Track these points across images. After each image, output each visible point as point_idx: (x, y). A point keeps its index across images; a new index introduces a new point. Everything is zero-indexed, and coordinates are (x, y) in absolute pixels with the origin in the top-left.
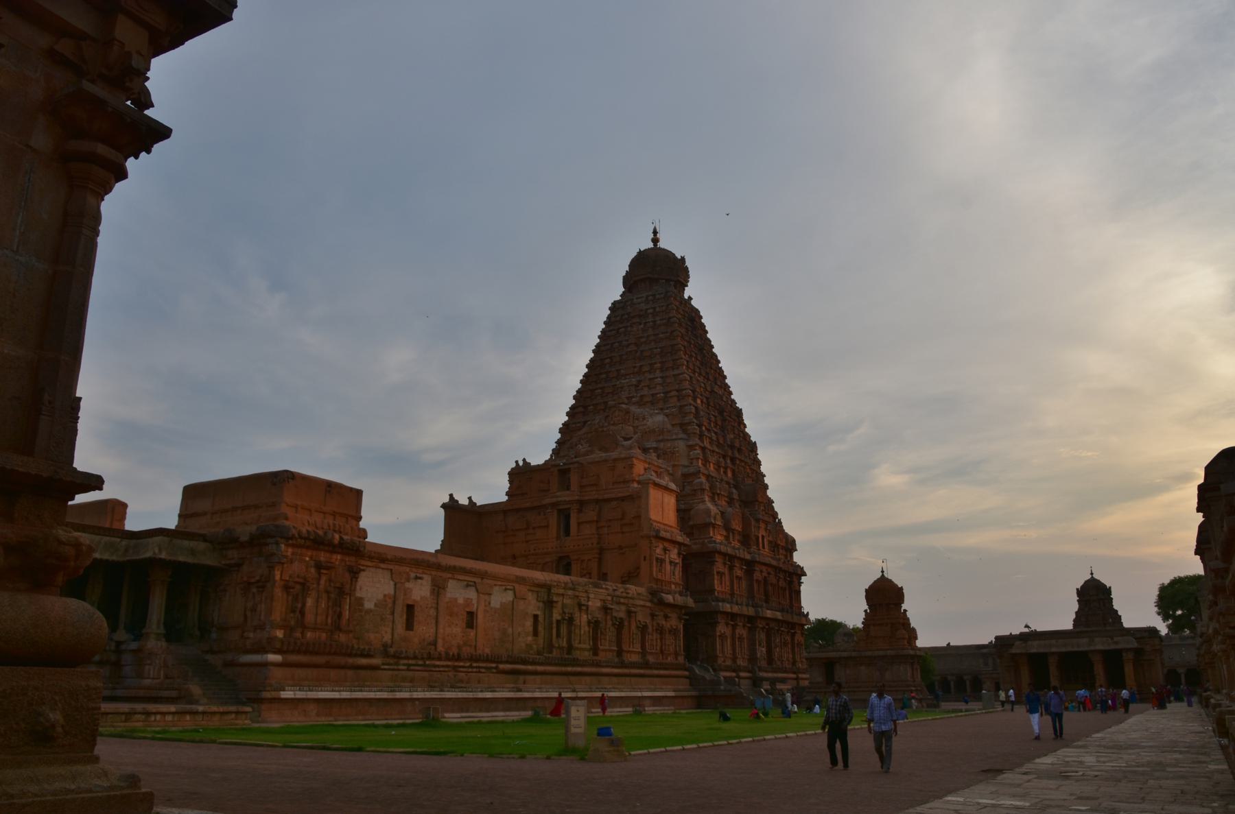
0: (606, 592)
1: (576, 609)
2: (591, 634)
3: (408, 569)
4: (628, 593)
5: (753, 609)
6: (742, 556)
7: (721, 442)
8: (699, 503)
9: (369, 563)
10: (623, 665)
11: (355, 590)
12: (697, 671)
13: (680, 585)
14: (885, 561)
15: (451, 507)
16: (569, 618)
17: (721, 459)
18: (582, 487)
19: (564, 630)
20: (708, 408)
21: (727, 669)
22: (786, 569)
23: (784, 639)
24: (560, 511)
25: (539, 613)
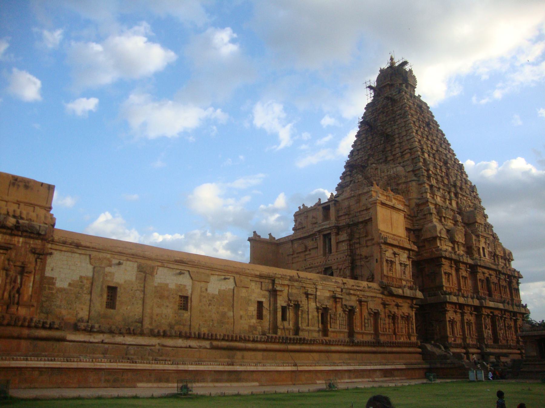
0: (336, 284)
1: (304, 298)
2: (320, 318)
3: (109, 256)
5: (478, 301)
6: (465, 261)
7: (446, 182)
9: (64, 249)
11: (43, 270)
13: (410, 281)
19: (290, 314)
20: (435, 161)
21: (457, 346)
22: (505, 272)
23: (508, 324)
24: (325, 236)
25: (263, 300)
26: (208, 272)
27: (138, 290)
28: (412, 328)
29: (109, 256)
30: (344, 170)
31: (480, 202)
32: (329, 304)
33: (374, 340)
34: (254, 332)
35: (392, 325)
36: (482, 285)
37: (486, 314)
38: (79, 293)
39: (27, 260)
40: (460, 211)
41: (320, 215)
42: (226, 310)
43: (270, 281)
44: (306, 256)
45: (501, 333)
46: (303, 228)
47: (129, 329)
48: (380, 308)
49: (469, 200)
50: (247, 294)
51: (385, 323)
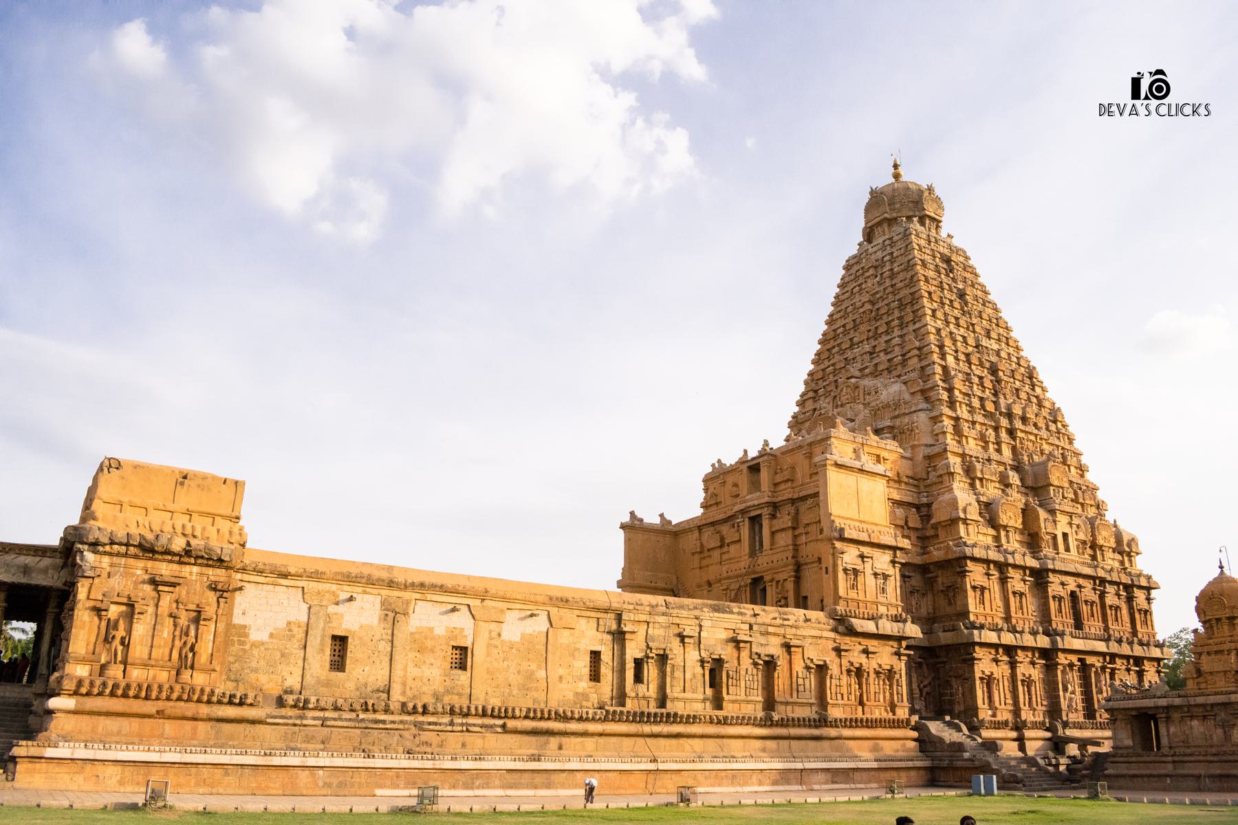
0: (740, 617)
3: (334, 587)
4: (788, 620)
5: (1047, 639)
11: (230, 614)
12: (933, 731)
13: (897, 606)
14: (1223, 549)
15: (633, 527)
18: (776, 485)
19: (651, 671)
28: (898, 693)
30: (802, 388)
31: (1071, 441)
33: (816, 717)
34: (585, 703)
35: (857, 687)
36: (1060, 605)
37: (1067, 662)
38: (286, 649)
39: (204, 601)
40: (1019, 463)
41: (743, 479)
42: (534, 667)
44: (723, 556)
46: (717, 504)
47: (366, 703)
48: (831, 659)
49: (1041, 439)
50: (571, 639)
51: (840, 684)
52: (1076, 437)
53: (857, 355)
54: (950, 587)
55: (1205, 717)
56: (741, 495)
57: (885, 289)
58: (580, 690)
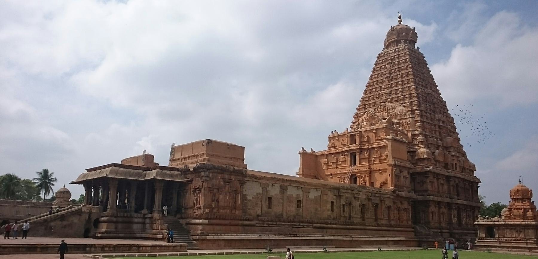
1: (353, 199)
2: (361, 210)
3: (268, 182)
4: (381, 192)
6: (443, 174)
8: (420, 148)
10: (378, 225)
11: (243, 191)
16: (349, 203)
17: (433, 127)
19: (346, 209)
25: (334, 201)
26: (309, 187)
27: (280, 198)
29: (268, 182)
32: (365, 202)
34: (331, 219)
37: (455, 208)
38: (257, 202)
43: (337, 190)
45: (464, 220)
46: (335, 147)
47: (279, 219)
48: (392, 205)
52: (457, 128)
53: (384, 93)
54: (421, 181)
55: (511, 229)
56: (347, 145)
57: (396, 69)
58: (329, 214)
